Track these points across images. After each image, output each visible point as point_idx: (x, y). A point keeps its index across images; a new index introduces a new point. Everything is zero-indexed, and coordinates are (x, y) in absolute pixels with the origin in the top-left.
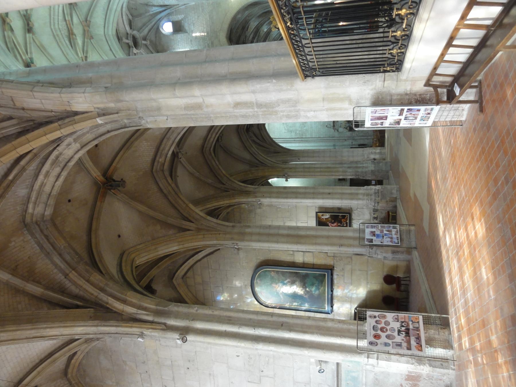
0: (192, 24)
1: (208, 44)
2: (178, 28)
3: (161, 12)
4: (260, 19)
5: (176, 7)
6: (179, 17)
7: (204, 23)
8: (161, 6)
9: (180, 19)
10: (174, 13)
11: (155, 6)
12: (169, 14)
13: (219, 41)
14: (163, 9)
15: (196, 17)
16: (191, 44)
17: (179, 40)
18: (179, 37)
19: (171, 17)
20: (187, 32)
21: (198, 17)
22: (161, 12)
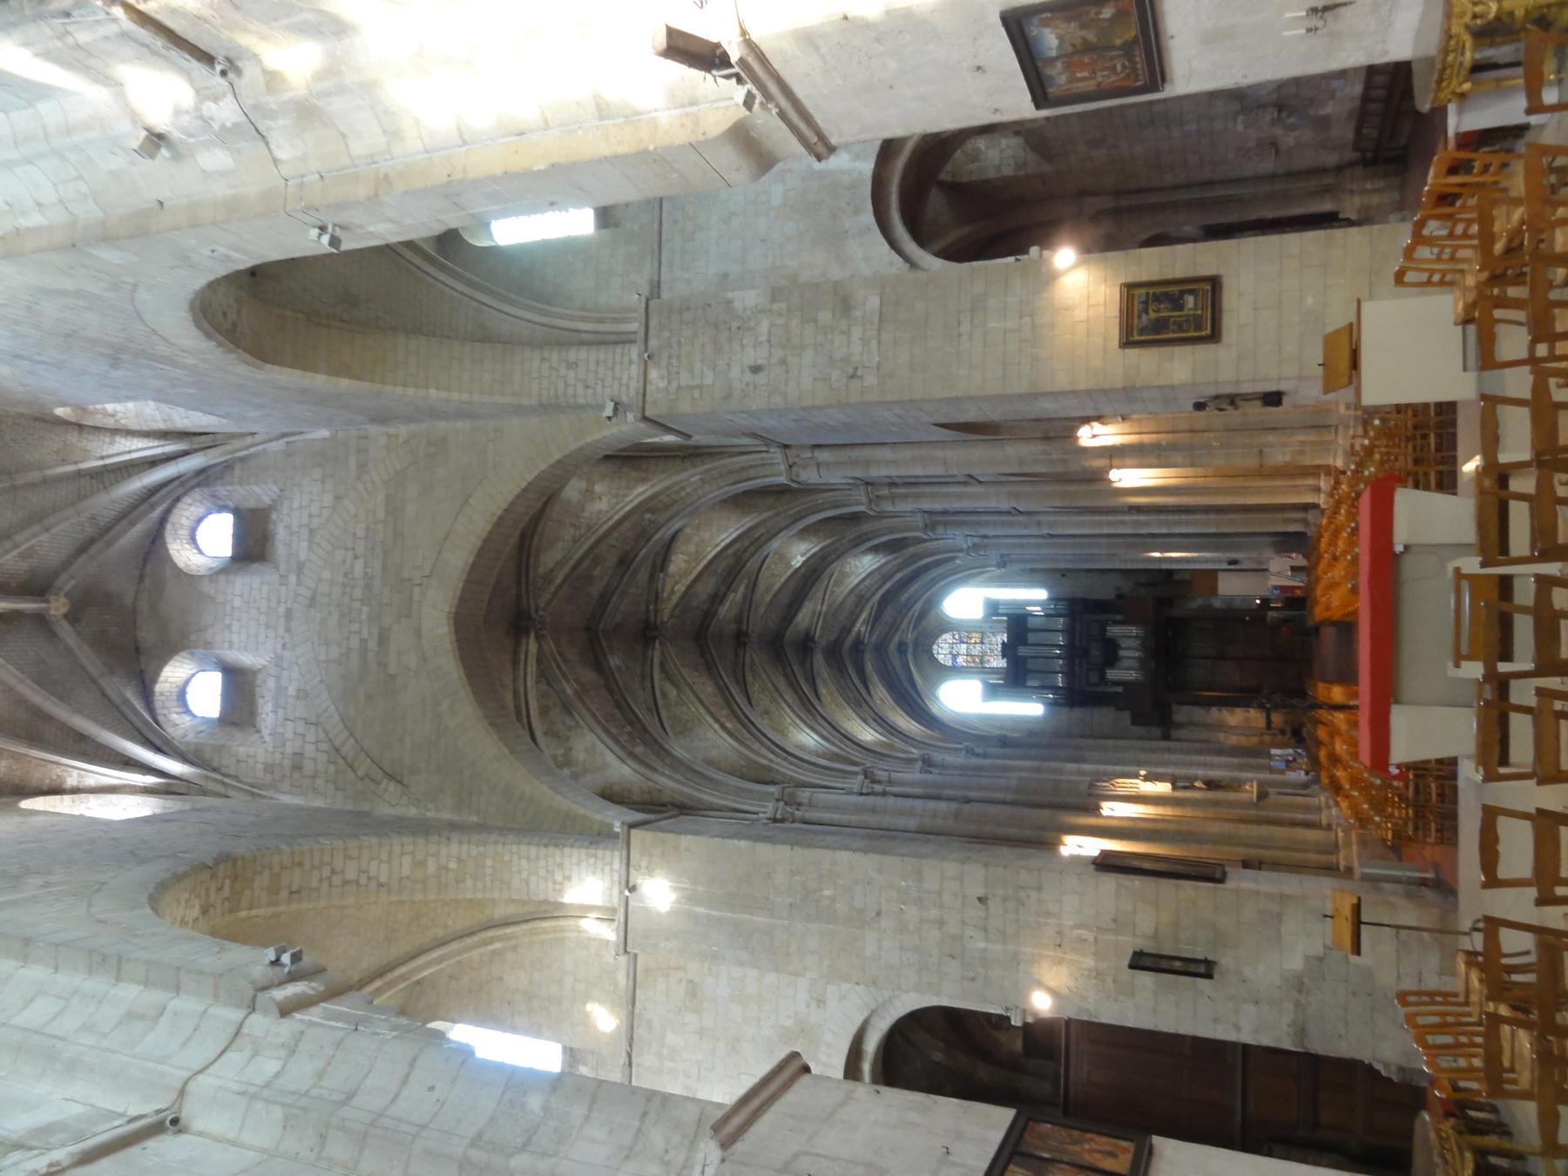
0: (305, 533)
1: (363, 642)
2: (253, 545)
3: (153, 463)
4: (747, 521)
5: (237, 444)
6: (260, 493)
7: (361, 533)
8: (164, 435)
9: (267, 500)
10: (237, 472)
11: (130, 433)
12: (202, 478)
13: (418, 632)
14: (170, 448)
15: (328, 499)
16: (288, 630)
17: (237, 602)
18: (251, 585)
19: (222, 491)
20: (276, 567)
21: (338, 498)
22: (153, 463)
